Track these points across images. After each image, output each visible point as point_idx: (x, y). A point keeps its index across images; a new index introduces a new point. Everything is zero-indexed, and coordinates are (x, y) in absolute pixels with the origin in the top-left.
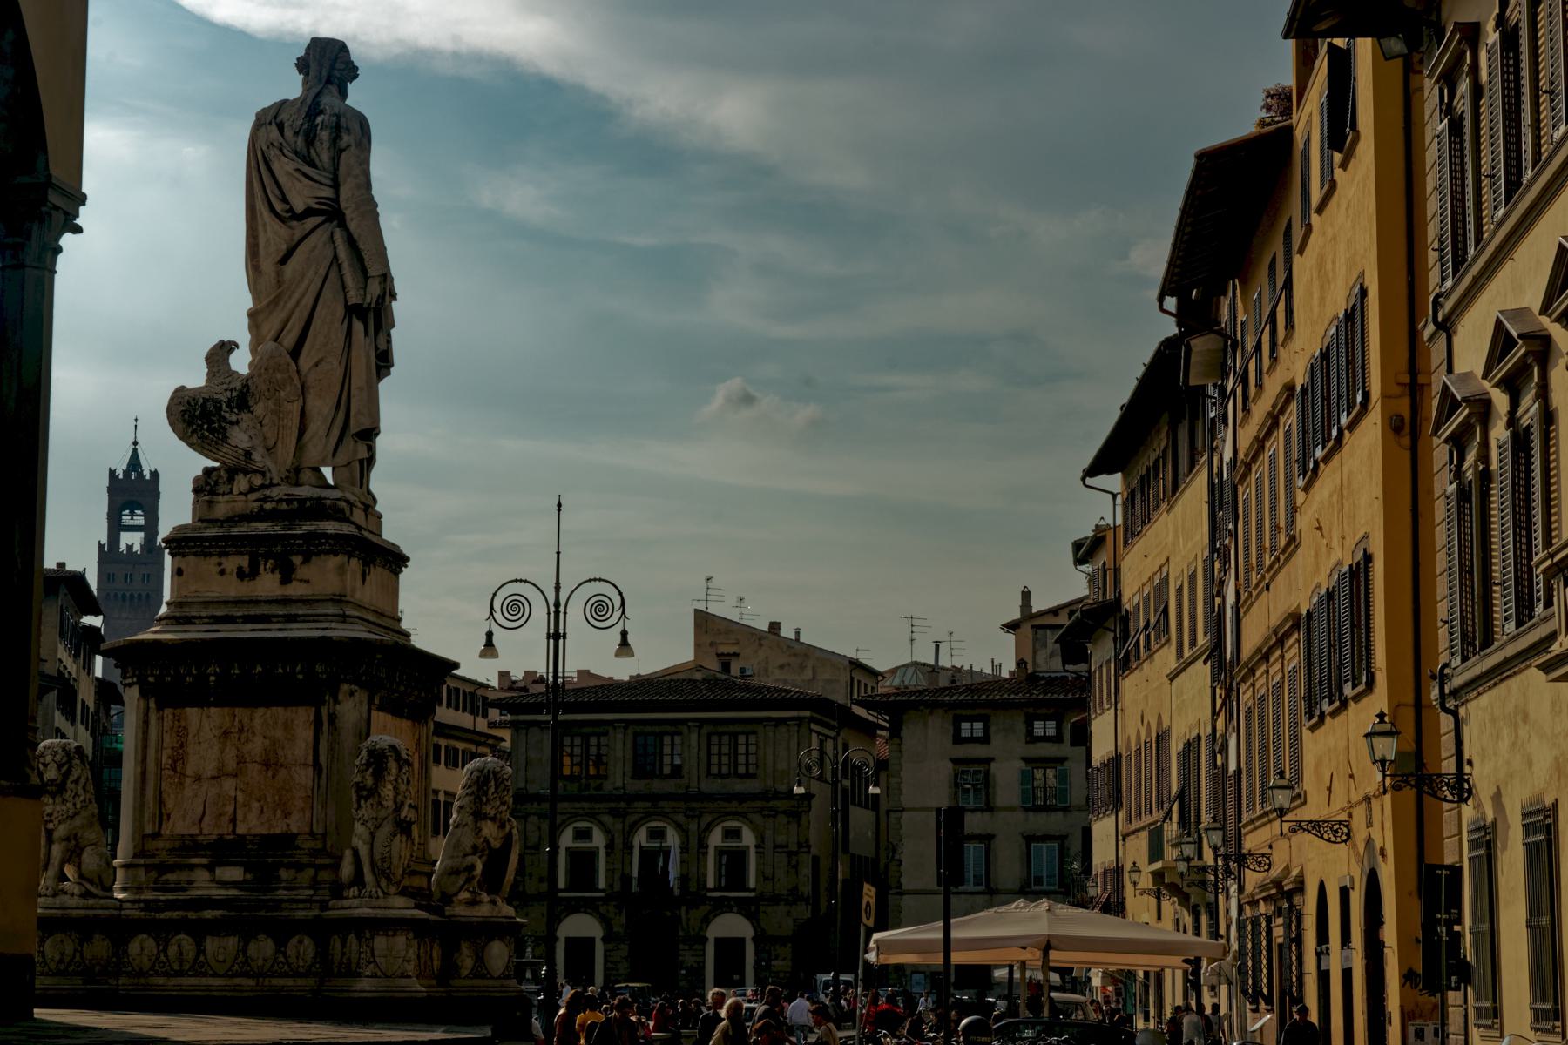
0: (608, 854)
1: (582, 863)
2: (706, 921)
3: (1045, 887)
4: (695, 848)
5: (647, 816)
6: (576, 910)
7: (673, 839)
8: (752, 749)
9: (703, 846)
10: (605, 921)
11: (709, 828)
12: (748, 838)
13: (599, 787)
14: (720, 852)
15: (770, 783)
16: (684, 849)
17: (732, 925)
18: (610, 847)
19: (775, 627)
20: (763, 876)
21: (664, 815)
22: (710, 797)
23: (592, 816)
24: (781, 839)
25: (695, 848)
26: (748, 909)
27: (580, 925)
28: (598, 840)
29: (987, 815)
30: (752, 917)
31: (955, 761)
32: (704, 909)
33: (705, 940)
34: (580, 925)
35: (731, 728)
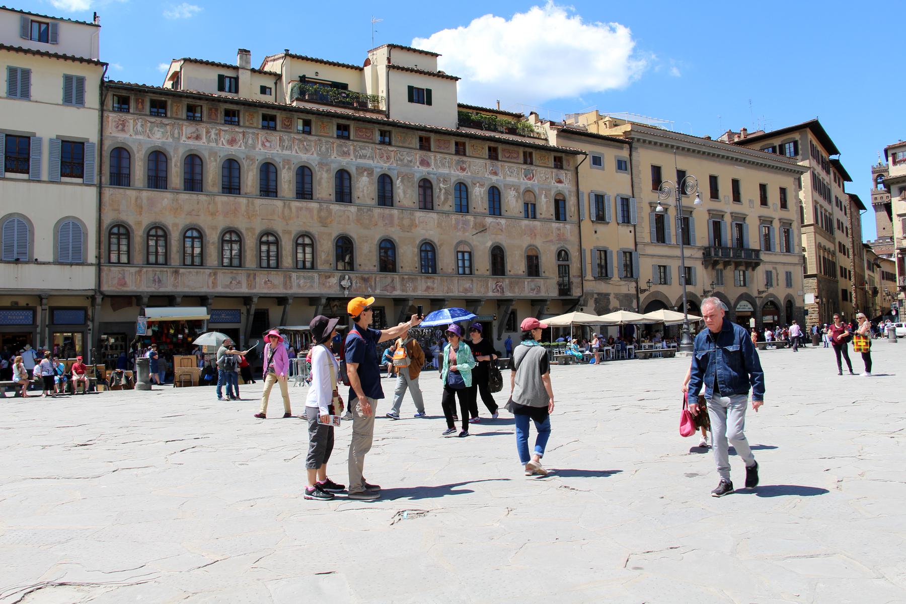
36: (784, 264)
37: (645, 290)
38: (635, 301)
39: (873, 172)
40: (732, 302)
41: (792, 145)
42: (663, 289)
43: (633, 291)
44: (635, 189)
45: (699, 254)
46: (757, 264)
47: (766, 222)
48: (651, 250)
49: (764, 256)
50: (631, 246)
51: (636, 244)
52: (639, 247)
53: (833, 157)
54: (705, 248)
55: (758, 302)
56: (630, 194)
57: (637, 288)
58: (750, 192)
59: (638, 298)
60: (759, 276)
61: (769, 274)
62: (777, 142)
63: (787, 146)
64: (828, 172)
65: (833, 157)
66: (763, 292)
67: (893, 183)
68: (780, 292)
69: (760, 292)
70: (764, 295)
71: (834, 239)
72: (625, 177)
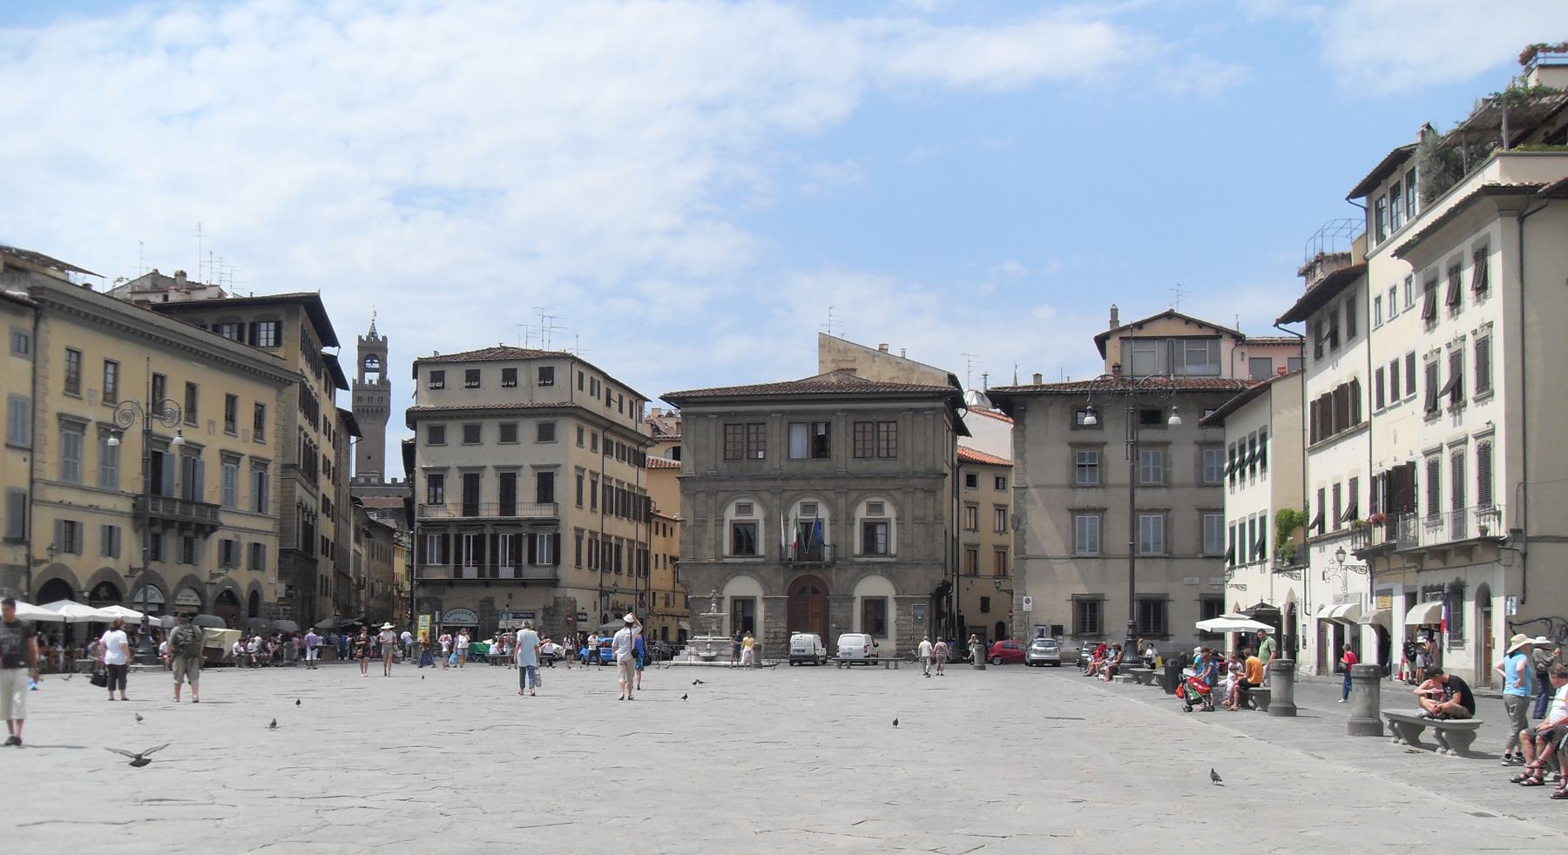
0: (766, 525)
1: (744, 540)
2: (854, 581)
3: (1152, 553)
4: (843, 520)
5: (802, 492)
7: (823, 513)
8: (892, 435)
9: (850, 521)
10: (764, 583)
11: (856, 503)
12: (889, 512)
15: (909, 464)
16: (834, 522)
17: (875, 586)
18: (768, 520)
19: (883, 349)
21: (817, 492)
22: (856, 477)
23: (753, 492)
24: (919, 512)
25: (843, 520)
27: (744, 586)
28: (758, 514)
29: (1100, 491)
30: (891, 578)
31: (1071, 445)
32: (852, 572)
33: (851, 599)
34: (744, 586)
35: (874, 417)
36: (252, 531)
37: (42, 562)
38: (24, 579)
39: (360, 348)
40: (171, 589)
41: (272, 326)
42: (67, 560)
43: (22, 562)
44: (39, 387)
45: (125, 506)
46: (214, 528)
47: (230, 458)
48: (53, 495)
49: (224, 518)
50: (23, 484)
51: (32, 482)
52: (37, 486)
53: (327, 350)
54: (136, 497)
55: (210, 591)
56: (28, 394)
57: (28, 557)
58: (211, 406)
59: (29, 574)
60: (210, 551)
61: (227, 546)
62: (247, 318)
63: (263, 326)
64: (318, 376)
65: (327, 350)
66: (219, 575)
67: (421, 418)
68: (242, 578)
69: (213, 576)
70: (218, 580)
71: (317, 488)
72: (24, 365)
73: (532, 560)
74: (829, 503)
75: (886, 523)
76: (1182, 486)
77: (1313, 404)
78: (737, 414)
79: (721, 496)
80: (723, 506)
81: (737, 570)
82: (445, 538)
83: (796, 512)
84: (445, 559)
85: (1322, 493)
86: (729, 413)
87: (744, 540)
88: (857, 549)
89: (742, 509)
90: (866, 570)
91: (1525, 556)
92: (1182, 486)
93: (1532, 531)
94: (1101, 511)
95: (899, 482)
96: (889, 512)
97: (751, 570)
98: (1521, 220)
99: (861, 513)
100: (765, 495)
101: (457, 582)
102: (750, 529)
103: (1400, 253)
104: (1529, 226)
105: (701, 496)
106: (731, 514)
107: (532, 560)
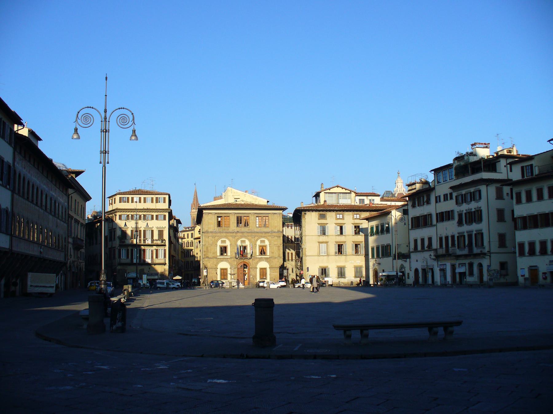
2: (257, 263)
5: (242, 237)
6: (222, 261)
8: (267, 221)
10: (230, 263)
11: (257, 240)
13: (228, 230)
14: (260, 246)
17: (263, 264)
20: (271, 252)
21: (245, 237)
22: (257, 233)
23: (226, 237)
24: (276, 243)
26: (267, 260)
30: (268, 262)
32: (256, 260)
35: (262, 215)
73: (157, 257)
74: (249, 240)
75: (266, 246)
76: (349, 235)
77: (412, 218)
78: (221, 213)
79: (216, 238)
80: (217, 241)
81: (222, 260)
82: (128, 250)
83: (259, 243)
84: (128, 257)
85: (416, 241)
86: (219, 213)
87: (224, 250)
88: (258, 253)
89: (223, 242)
90: (261, 259)
91: (490, 257)
92: (349, 235)
93: (491, 251)
94: (327, 242)
95: (269, 234)
96: (267, 243)
97: (226, 260)
98: (487, 186)
99: (259, 243)
100: (230, 238)
101: (132, 264)
102: (264, 248)
103: (451, 188)
104: (488, 187)
105: (210, 238)
106: (219, 243)
107: (157, 257)
